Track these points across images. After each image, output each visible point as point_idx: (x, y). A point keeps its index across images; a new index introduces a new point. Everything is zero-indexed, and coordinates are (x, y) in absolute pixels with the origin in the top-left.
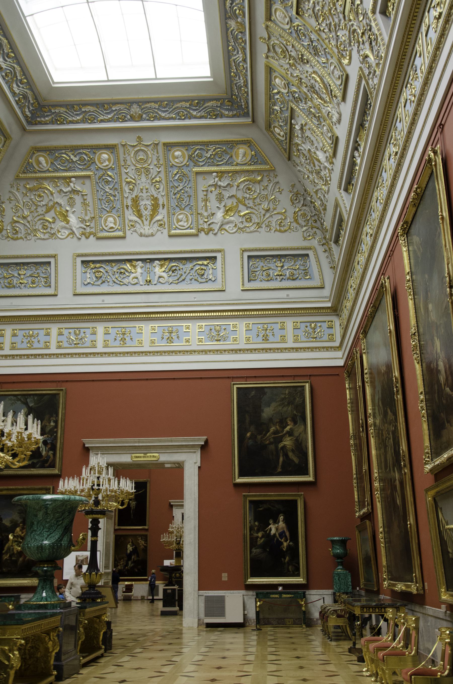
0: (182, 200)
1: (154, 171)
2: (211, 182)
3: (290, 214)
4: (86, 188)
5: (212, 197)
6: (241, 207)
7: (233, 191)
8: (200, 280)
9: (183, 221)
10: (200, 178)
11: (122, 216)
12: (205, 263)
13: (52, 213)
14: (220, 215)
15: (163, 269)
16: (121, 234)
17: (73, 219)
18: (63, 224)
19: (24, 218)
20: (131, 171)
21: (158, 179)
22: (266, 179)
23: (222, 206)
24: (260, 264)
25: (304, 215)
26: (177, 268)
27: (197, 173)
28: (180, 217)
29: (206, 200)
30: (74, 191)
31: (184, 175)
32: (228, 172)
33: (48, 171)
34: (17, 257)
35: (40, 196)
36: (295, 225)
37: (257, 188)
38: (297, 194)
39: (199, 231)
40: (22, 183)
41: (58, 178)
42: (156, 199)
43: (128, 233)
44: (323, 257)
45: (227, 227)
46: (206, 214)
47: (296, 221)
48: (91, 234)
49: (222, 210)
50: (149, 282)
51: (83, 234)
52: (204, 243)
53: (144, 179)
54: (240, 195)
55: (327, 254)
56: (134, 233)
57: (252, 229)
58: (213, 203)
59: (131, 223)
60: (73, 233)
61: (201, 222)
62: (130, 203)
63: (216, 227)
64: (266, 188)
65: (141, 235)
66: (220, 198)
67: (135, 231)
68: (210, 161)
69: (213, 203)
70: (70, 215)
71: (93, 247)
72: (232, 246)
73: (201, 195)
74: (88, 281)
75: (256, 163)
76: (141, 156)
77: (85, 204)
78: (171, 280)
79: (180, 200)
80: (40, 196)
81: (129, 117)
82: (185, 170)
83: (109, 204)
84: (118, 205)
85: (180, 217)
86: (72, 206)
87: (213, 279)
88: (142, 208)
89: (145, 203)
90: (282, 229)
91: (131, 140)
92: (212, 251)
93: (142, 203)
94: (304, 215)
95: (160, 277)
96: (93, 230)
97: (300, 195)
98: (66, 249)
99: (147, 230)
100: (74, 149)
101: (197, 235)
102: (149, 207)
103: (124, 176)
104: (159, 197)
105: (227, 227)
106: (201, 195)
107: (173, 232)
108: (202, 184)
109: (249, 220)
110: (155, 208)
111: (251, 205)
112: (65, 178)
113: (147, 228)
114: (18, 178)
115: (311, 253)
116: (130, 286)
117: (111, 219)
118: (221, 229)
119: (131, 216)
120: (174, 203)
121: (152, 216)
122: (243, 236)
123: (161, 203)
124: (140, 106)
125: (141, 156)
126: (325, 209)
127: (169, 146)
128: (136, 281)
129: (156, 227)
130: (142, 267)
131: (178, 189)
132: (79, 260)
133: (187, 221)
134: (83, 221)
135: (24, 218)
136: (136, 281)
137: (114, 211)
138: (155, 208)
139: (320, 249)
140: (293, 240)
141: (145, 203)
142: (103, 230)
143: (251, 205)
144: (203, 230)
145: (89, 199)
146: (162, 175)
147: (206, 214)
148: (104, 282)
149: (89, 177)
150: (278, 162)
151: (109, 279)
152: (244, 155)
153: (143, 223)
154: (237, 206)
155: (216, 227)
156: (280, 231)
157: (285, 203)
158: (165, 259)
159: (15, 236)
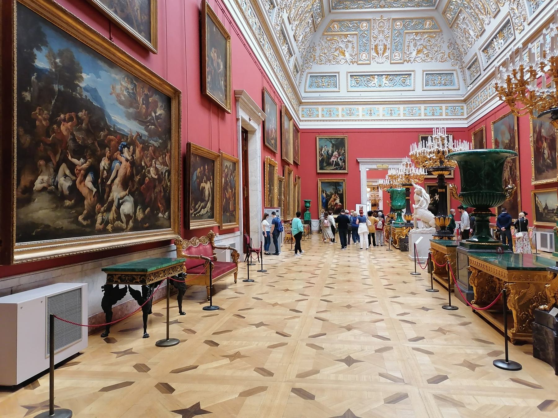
0: (398, 47)
1: (386, 31)
2: (412, 38)
3: (447, 53)
4: (354, 40)
5: (412, 45)
6: (424, 50)
7: (422, 42)
9: (397, 56)
10: (407, 35)
11: (369, 54)
13: (338, 52)
14: (414, 53)
16: (368, 62)
17: (347, 54)
18: (343, 57)
19: (325, 54)
20: (376, 32)
22: (437, 36)
23: (416, 49)
24: (430, 77)
25: (453, 54)
28: (396, 54)
29: (408, 46)
30: (349, 41)
31: (400, 34)
32: (421, 33)
33: (338, 31)
34: (322, 73)
35: (333, 43)
36: (448, 58)
37: (433, 41)
38: (451, 43)
39: (404, 61)
40: (325, 37)
41: (342, 35)
42: (385, 46)
43: (372, 61)
44: (460, 74)
45: (417, 59)
46: (408, 53)
47: (449, 57)
48: (355, 62)
49: (416, 51)
51: (352, 62)
52: (406, 67)
53: (381, 35)
54: (424, 44)
55: (462, 73)
57: (429, 60)
58: (412, 47)
60: (347, 62)
61: (405, 57)
62: (374, 47)
63: (412, 59)
64: (437, 41)
65: (378, 63)
66: (415, 45)
68: (414, 28)
69: (412, 47)
70: (346, 52)
71: (355, 68)
72: (418, 68)
73: (407, 44)
75: (434, 29)
77: (353, 48)
78: (390, 85)
79: (397, 46)
80: (333, 43)
82: (401, 31)
83: (365, 47)
84: (368, 48)
85: (396, 54)
86: (347, 48)
88: (379, 49)
89: (381, 47)
90: (443, 61)
92: (410, 71)
93: (379, 47)
94: (453, 54)
96: (356, 60)
97: (453, 44)
98: (343, 69)
99: (380, 60)
101: (403, 63)
102: (382, 50)
103: (372, 34)
104: (387, 44)
105: (417, 59)
106: (407, 44)
107: (392, 62)
108: (408, 38)
109: (428, 56)
110: (385, 49)
111: (429, 49)
112: (345, 35)
113: (380, 59)
114: (323, 35)
115: (454, 72)
117: (364, 55)
118: (414, 60)
119: (373, 53)
120: (394, 47)
121: (383, 54)
122: (424, 63)
123: (388, 47)
126: (466, 54)
129: (385, 59)
134: (351, 55)
135: (325, 54)
138: (385, 49)
139: (459, 71)
140: (446, 66)
141: (381, 47)
142: (360, 60)
143: (429, 49)
144: (406, 60)
145: (355, 45)
146: (390, 34)
147: (408, 53)
149: (356, 34)
150: (444, 28)
152: (430, 25)
154: (423, 49)
155: (412, 59)
156: (442, 62)
157: (445, 46)
158: (388, 75)
159: (321, 62)
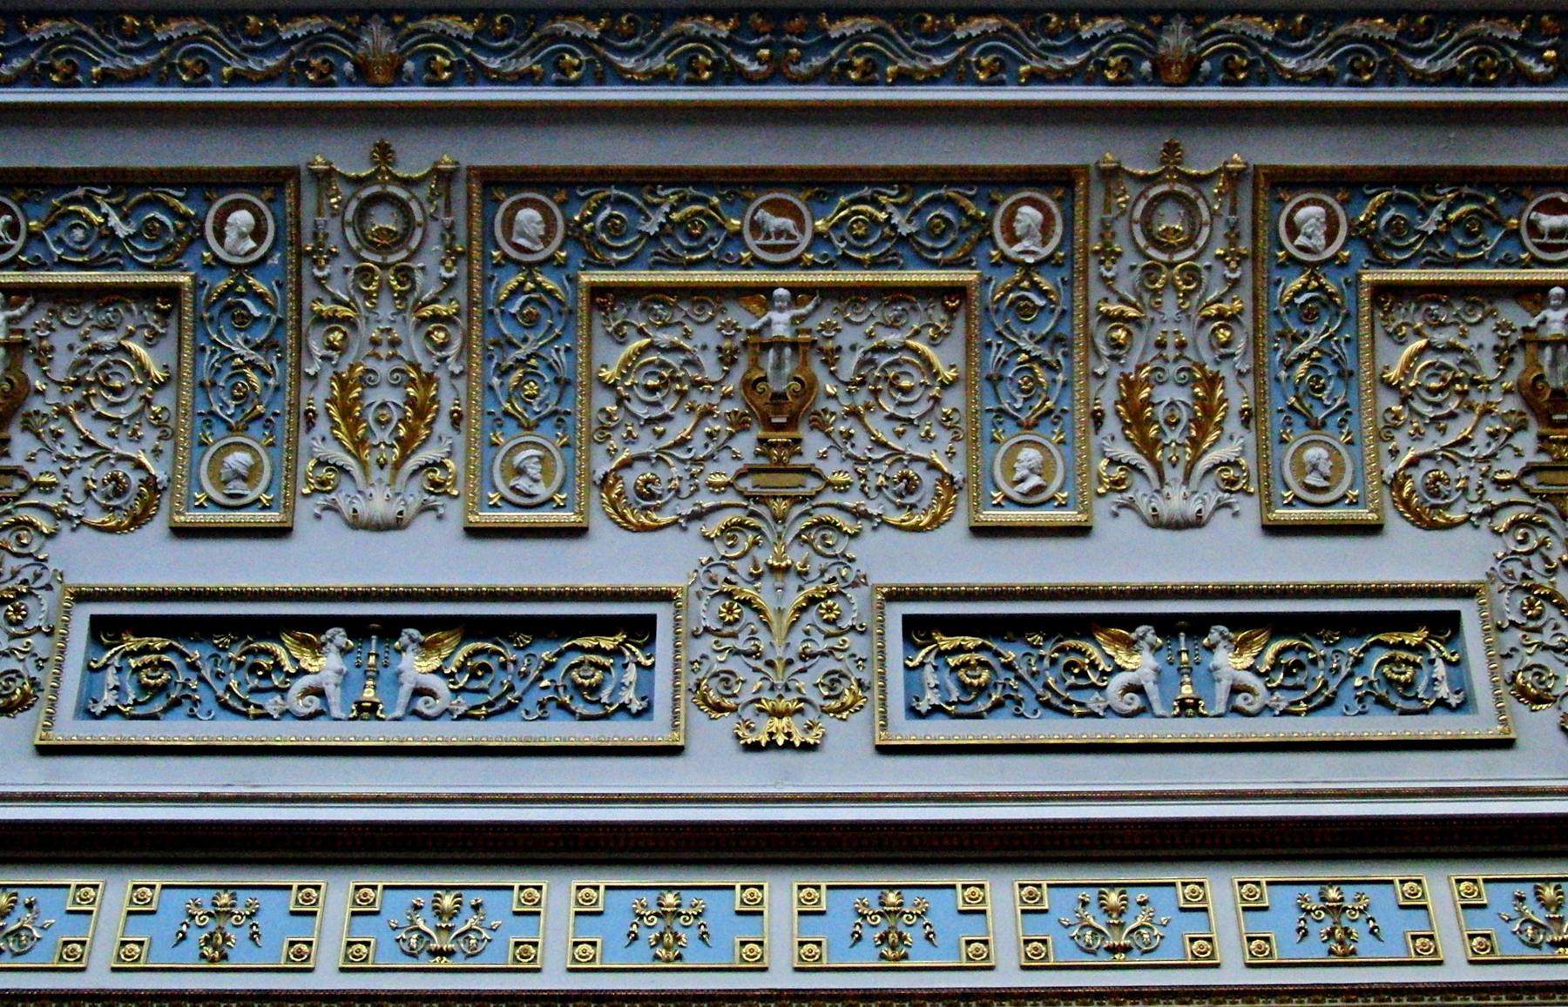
8: (580, 708)
12: (607, 643)
15: (435, 662)
16: (272, 517)
21: (442, 308)
26: (493, 663)
27: (597, 290)
43: (305, 509)
50: (368, 711)
56: (328, 515)
59: (323, 473)
67: (332, 508)
74: (109, 699)
76: (384, 220)
81: (348, 67)
87: (635, 707)
91: (348, 156)
95: (419, 692)
100: (120, 182)
116: (288, 723)
119: (323, 443)
124: (395, 28)
125: (384, 220)
127: (495, 182)
128: (316, 703)
129: (415, 494)
130: (344, 652)
131: (520, 354)
132: (83, 614)
133: (547, 473)
136: (316, 703)
137: (256, 428)
148: (176, 703)
151: (203, 694)
153: (366, 474)
